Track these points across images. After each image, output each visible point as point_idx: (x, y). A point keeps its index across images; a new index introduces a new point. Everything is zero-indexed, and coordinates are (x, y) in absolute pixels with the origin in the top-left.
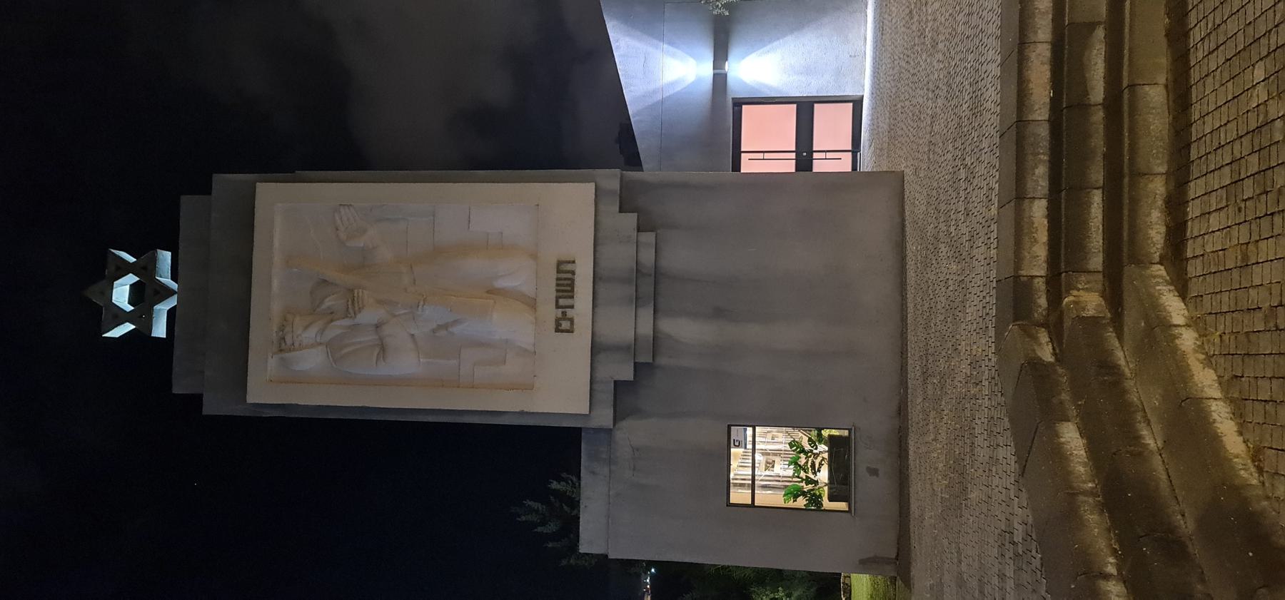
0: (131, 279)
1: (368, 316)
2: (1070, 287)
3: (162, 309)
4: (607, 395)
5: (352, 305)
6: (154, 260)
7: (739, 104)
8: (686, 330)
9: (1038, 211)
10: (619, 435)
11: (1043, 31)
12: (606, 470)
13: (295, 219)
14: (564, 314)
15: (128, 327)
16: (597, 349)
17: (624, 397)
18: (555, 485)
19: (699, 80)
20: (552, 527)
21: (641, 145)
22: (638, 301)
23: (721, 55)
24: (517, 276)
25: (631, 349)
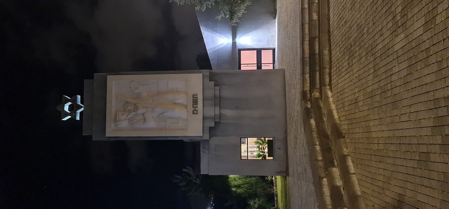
0: (70, 103)
1: (140, 111)
2: (313, 92)
3: (79, 111)
5: (136, 108)
6: (76, 98)
7: (240, 50)
8: (228, 112)
9: (307, 76)
10: (211, 142)
11: (307, 38)
12: (207, 151)
14: (195, 109)
15: (69, 117)
16: (204, 118)
17: (212, 131)
18: (184, 170)
19: (228, 44)
21: (212, 63)
22: (215, 105)
23: (234, 37)
24: (182, 99)
25: (214, 118)
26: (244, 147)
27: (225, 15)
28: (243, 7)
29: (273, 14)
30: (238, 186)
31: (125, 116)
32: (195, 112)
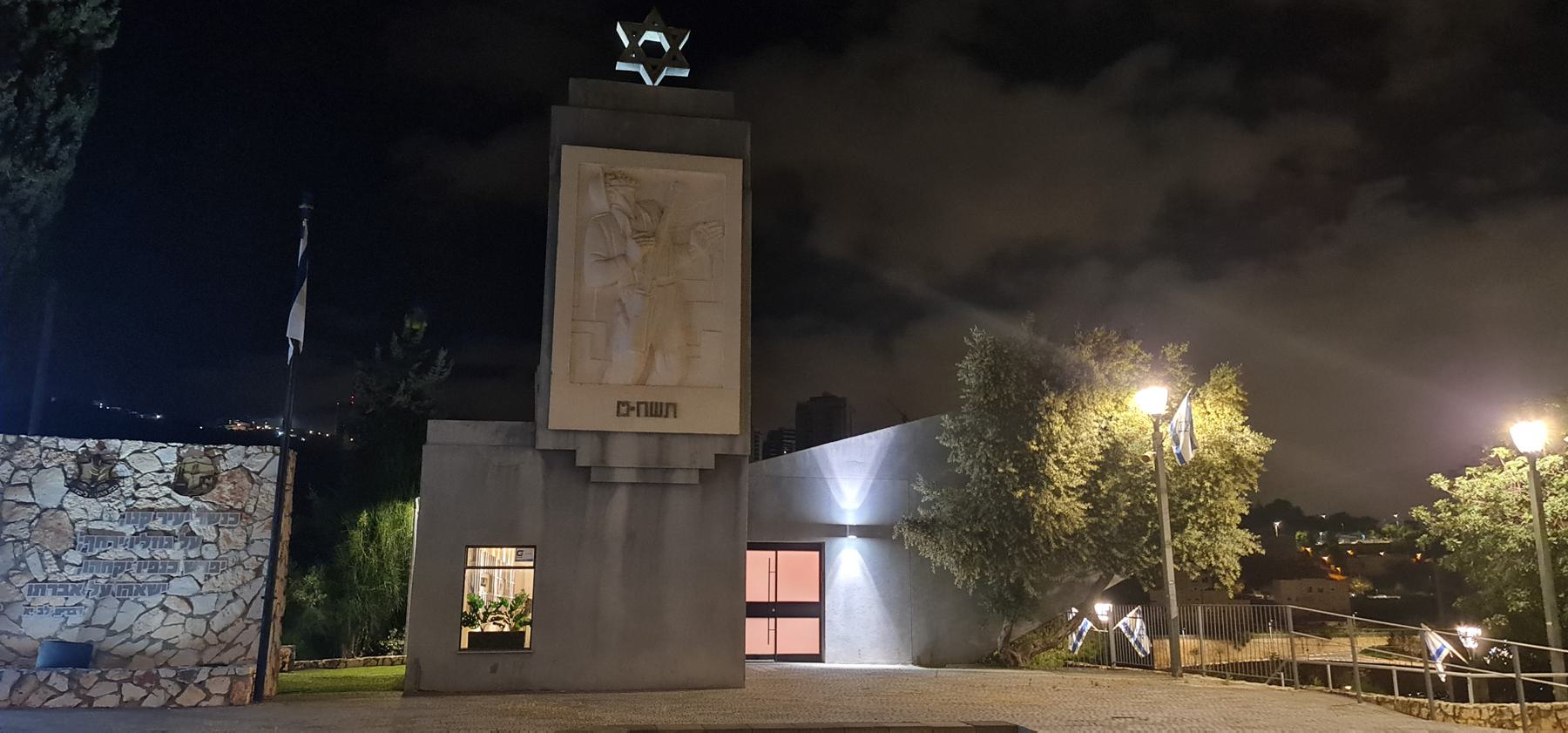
0: (667, 47)
3: (642, 70)
4: (564, 444)
5: (642, 236)
6: (682, 66)
7: (819, 548)
8: (618, 507)
10: (530, 453)
13: (709, 194)
15: (626, 43)
16: (603, 436)
17: (562, 460)
18: (443, 354)
19: (842, 512)
20: (397, 351)
21: (785, 459)
22: (642, 470)
23: (863, 531)
24: (666, 372)
25: (604, 466)
26: (507, 555)
27: (927, 505)
28: (949, 562)
29: (930, 658)
30: (373, 534)
31: (621, 202)
32: (623, 409)
